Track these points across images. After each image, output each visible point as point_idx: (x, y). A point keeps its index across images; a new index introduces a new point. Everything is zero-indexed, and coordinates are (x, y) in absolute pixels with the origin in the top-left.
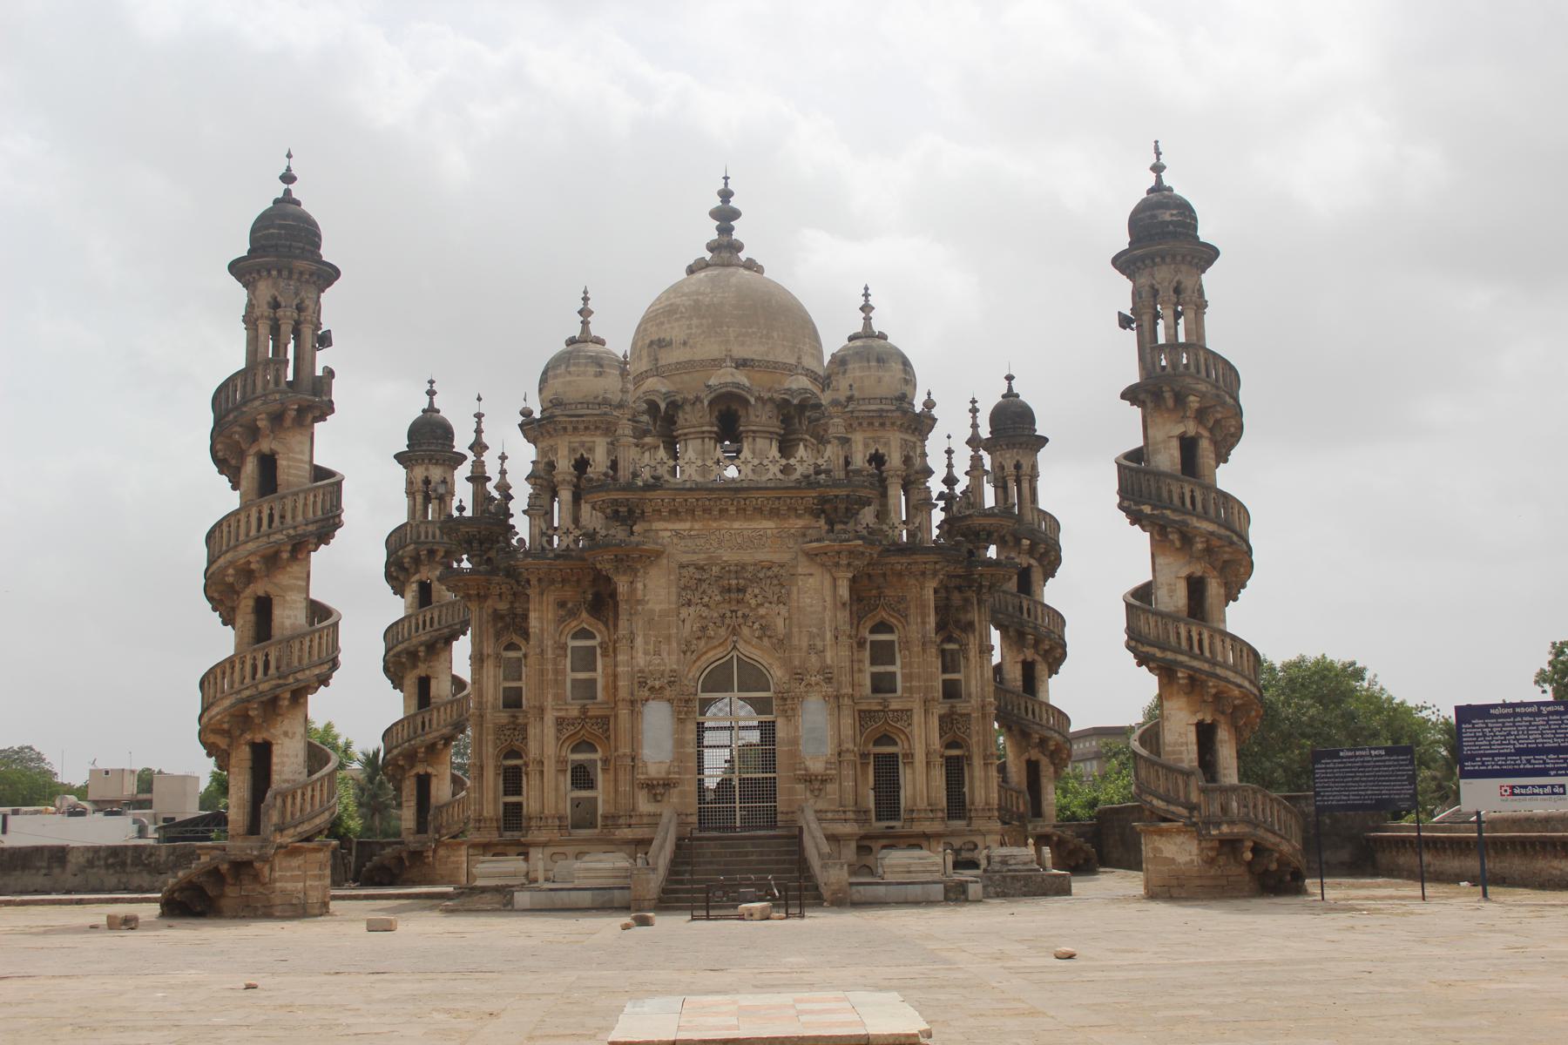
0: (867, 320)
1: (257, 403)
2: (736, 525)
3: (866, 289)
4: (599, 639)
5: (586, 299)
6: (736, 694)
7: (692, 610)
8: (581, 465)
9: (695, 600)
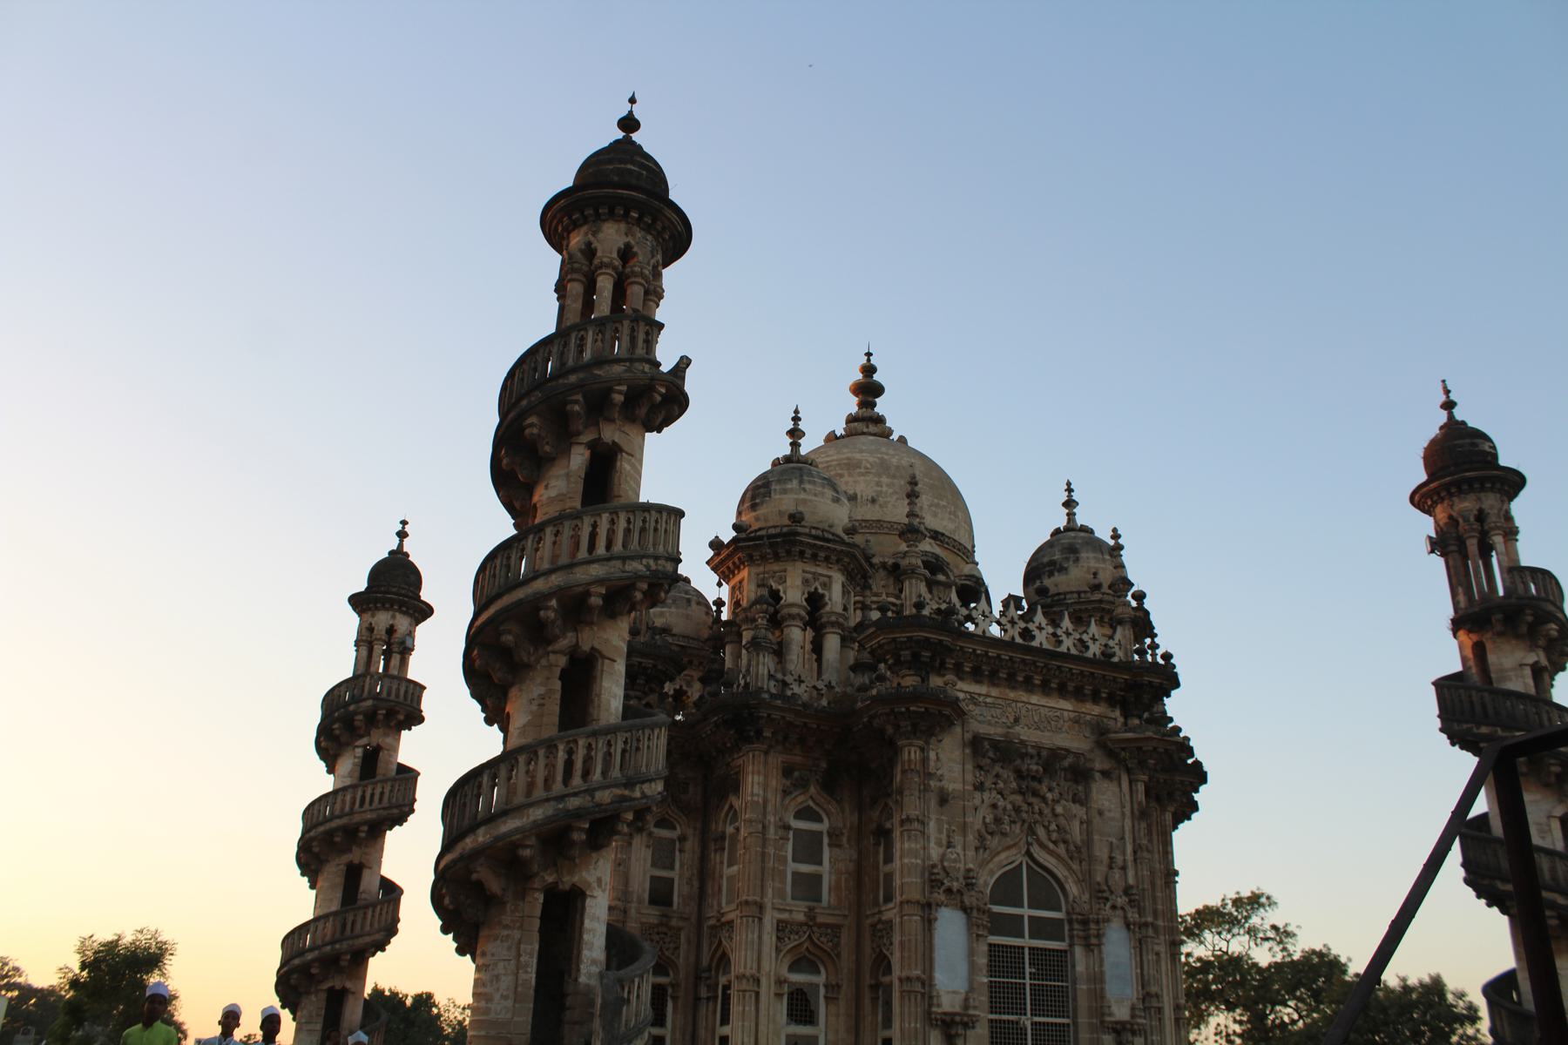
0: (1071, 516)
1: (618, 369)
2: (1034, 699)
3: (1069, 484)
4: (826, 820)
5: (796, 419)
6: (1026, 912)
7: (986, 795)
8: (815, 601)
9: (988, 784)
